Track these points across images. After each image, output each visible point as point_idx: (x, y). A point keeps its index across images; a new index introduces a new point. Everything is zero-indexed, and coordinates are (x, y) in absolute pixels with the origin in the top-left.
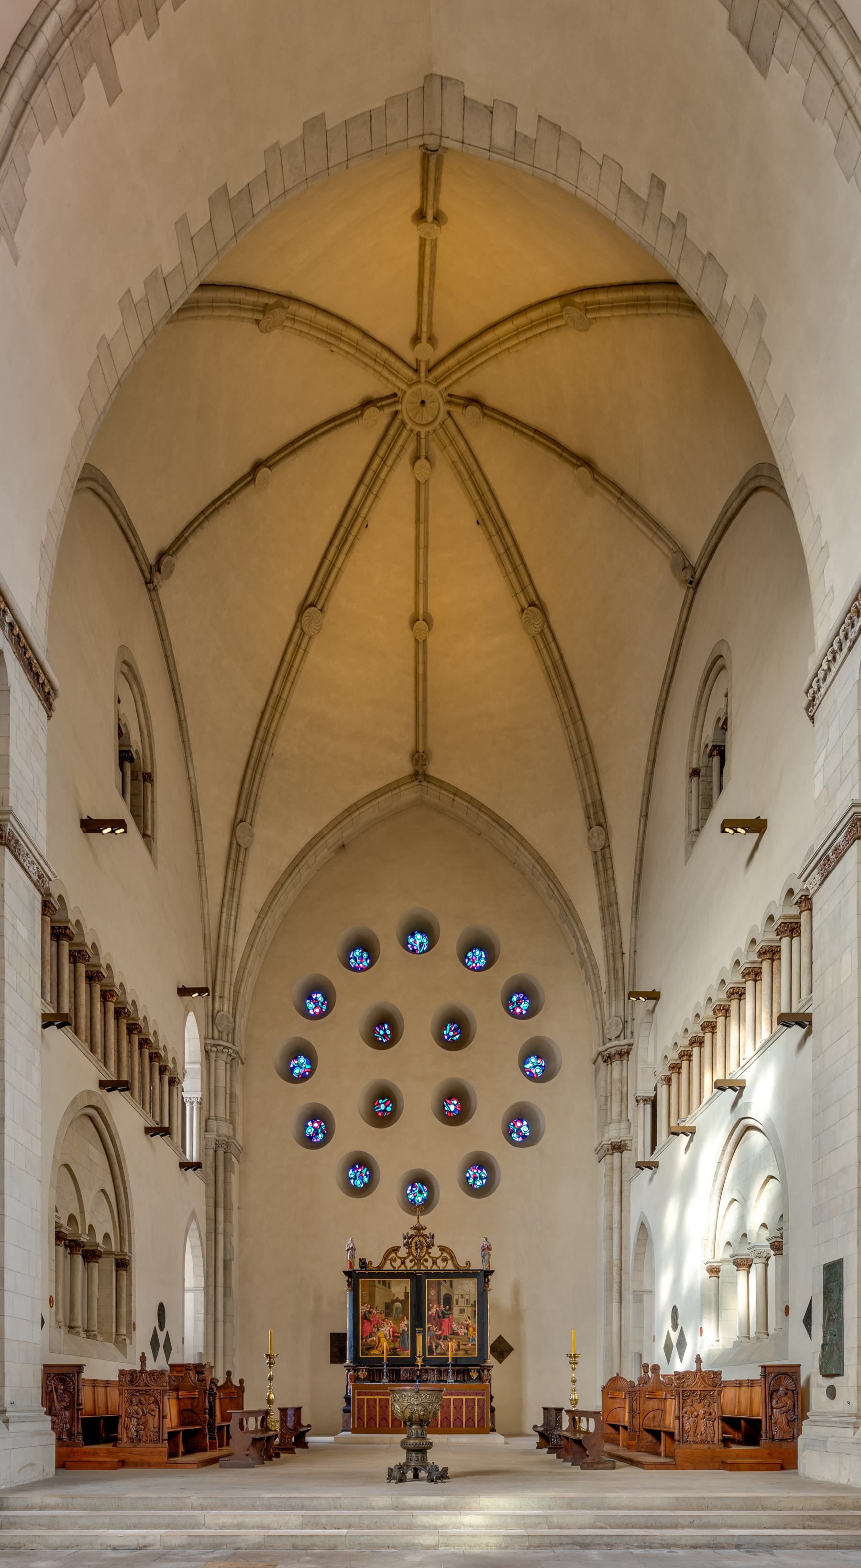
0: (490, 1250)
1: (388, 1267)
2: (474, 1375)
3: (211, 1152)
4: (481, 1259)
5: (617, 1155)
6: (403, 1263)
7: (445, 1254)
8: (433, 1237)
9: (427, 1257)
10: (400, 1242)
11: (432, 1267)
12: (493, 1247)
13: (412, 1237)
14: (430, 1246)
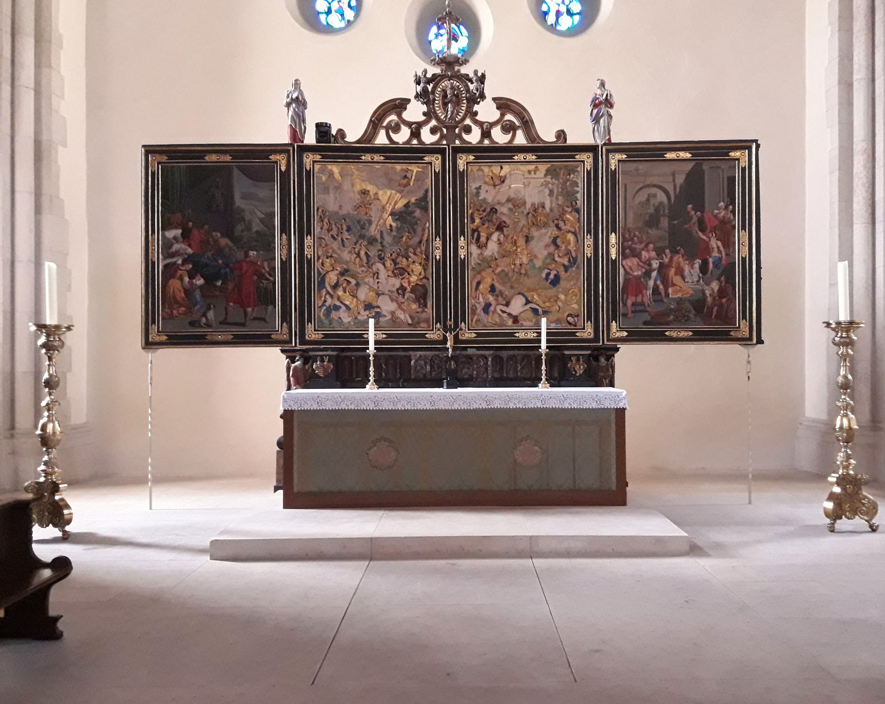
0: (611, 106)
1: (381, 139)
2: (580, 369)
4: (590, 125)
6: (416, 134)
7: (509, 117)
8: (482, 79)
9: (468, 121)
10: (409, 90)
11: (481, 141)
12: (615, 99)
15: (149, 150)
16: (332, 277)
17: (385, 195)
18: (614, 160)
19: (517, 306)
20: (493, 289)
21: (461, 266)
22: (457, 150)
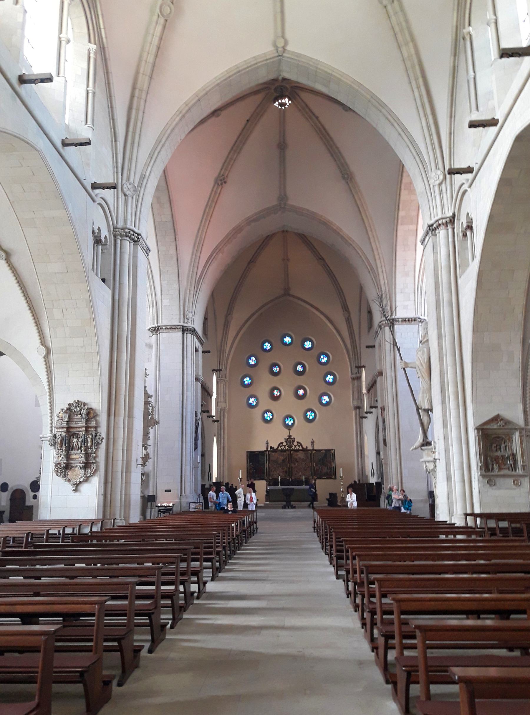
1: (280, 448)
3: (219, 413)
5: (358, 410)
6: (285, 447)
8: (294, 439)
10: (283, 441)
13: (288, 439)
14: (294, 441)
15: (247, 452)
16: (273, 470)
17: (281, 457)
18: (314, 452)
19: (300, 473)
20: (297, 471)
21: (292, 468)
22: (291, 450)
